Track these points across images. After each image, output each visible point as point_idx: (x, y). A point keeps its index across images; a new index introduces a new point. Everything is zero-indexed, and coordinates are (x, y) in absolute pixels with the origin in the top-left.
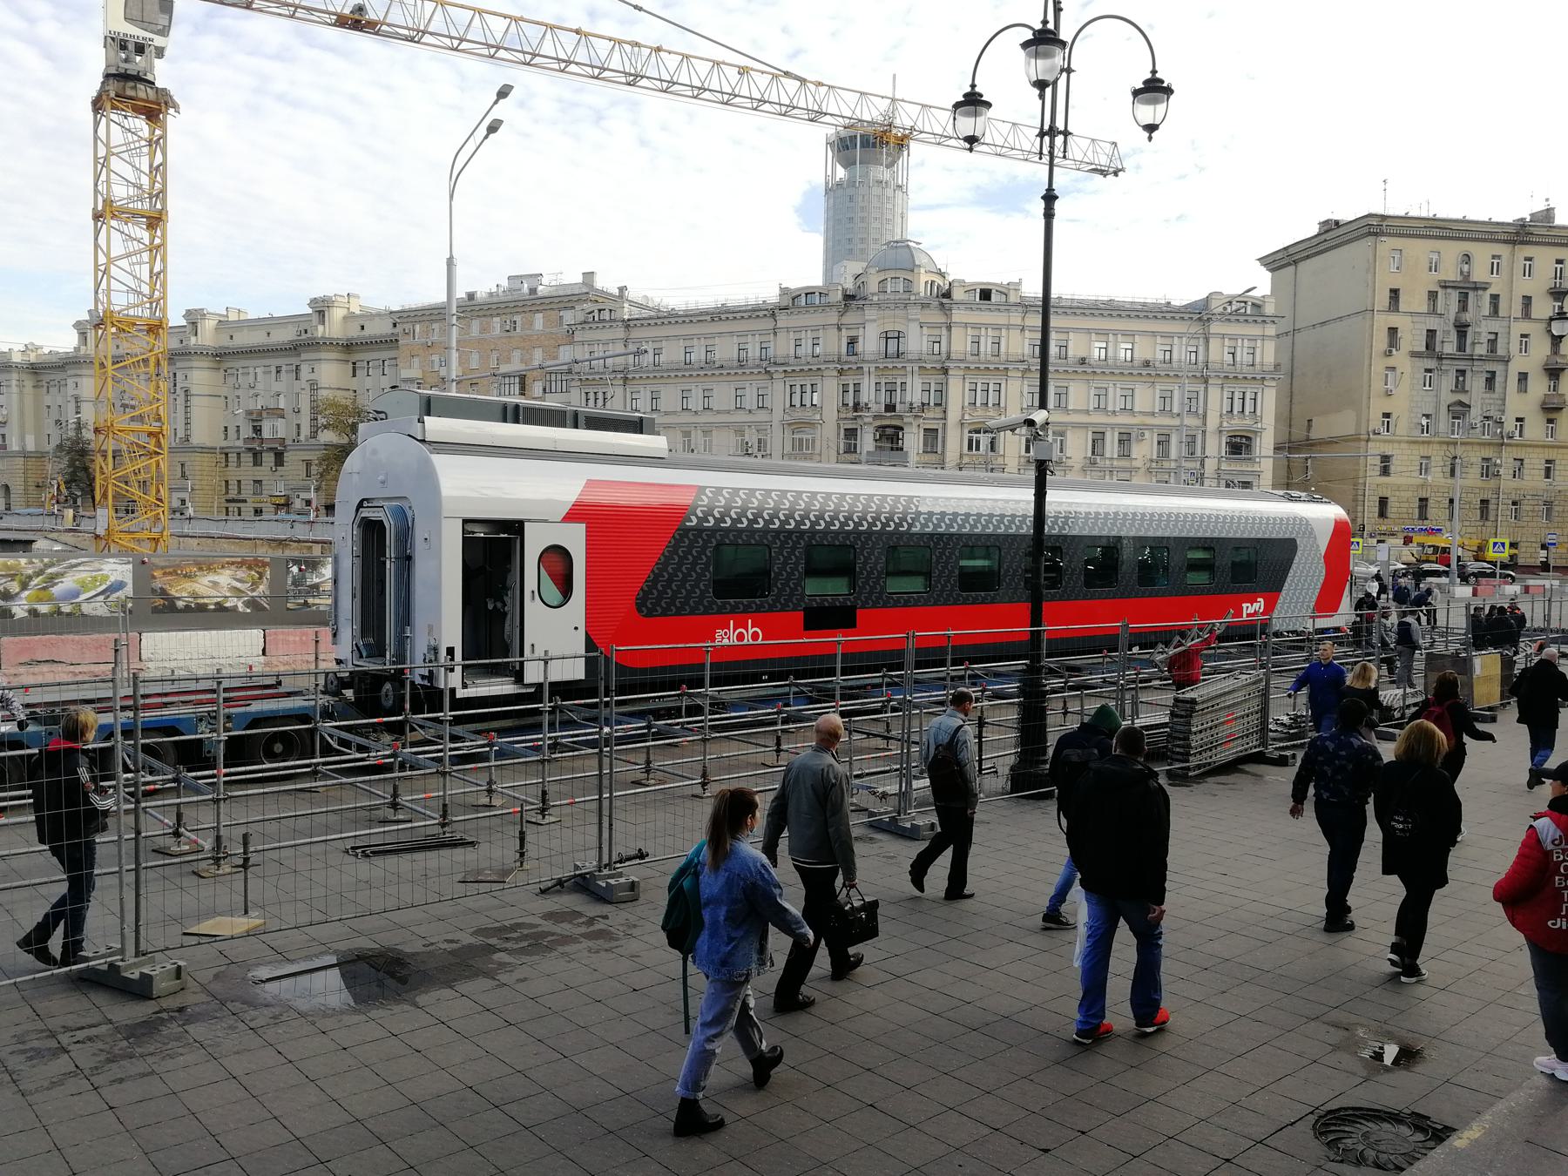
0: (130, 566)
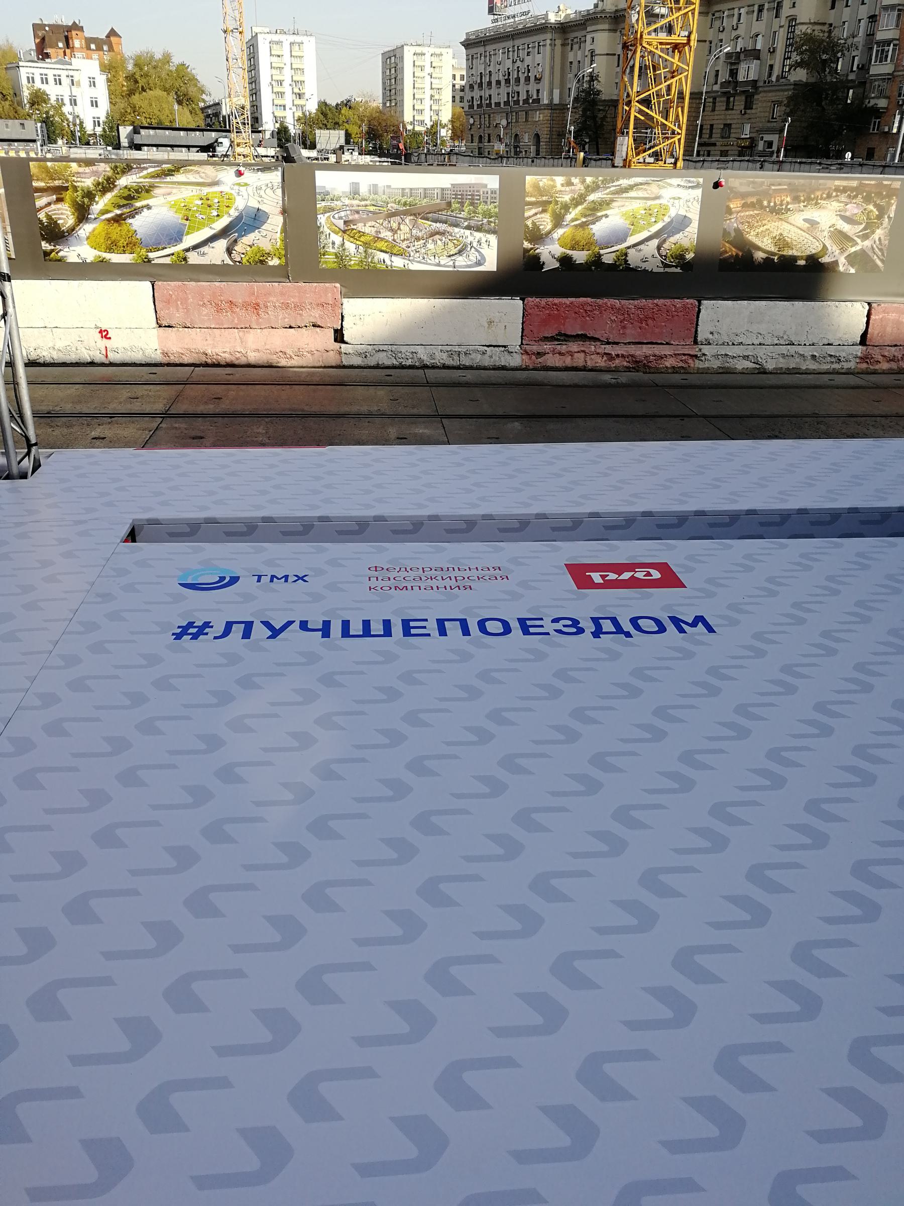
0: (698, 192)
